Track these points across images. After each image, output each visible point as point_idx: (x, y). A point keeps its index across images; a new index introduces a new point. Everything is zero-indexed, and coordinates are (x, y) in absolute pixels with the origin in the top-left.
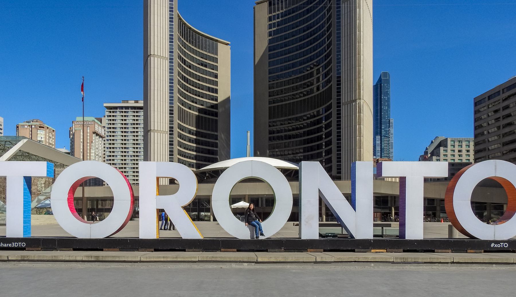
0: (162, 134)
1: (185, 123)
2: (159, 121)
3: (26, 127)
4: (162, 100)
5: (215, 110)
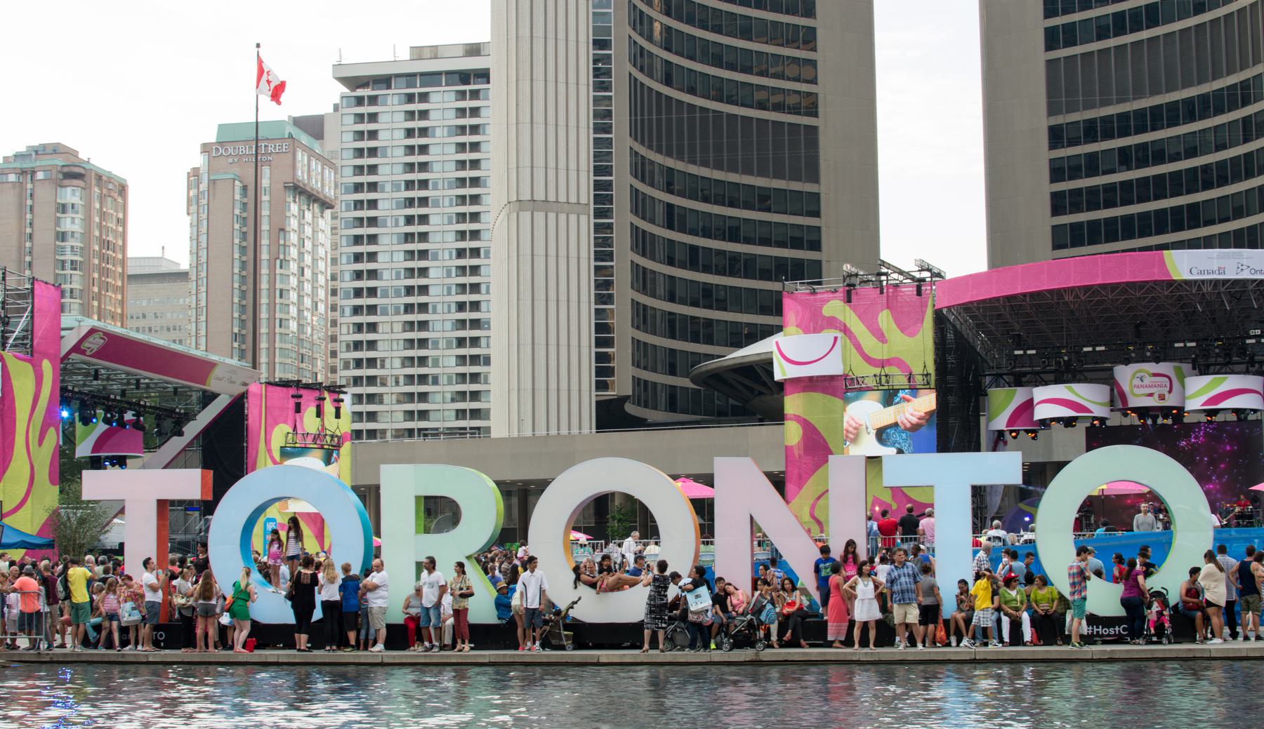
0: (563, 217)
1: (669, 154)
2: (552, 164)
4: (562, 78)
5: (804, 87)
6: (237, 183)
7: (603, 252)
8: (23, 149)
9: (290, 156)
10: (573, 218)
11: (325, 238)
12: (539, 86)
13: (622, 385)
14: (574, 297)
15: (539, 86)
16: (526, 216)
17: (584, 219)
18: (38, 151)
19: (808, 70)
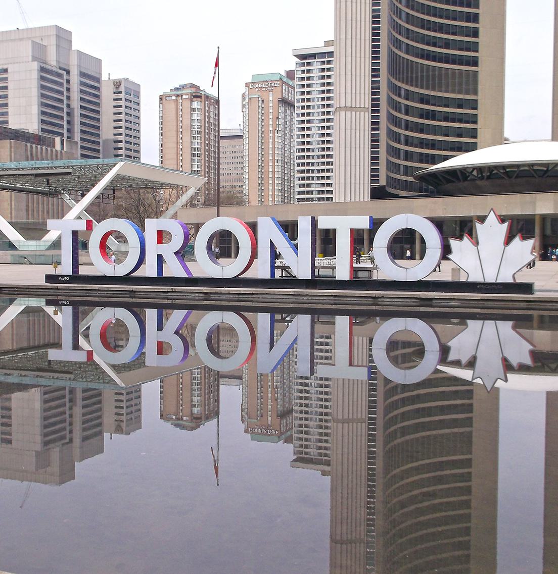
0: (358, 113)
2: (354, 91)
3: (173, 98)
6: (260, 99)
8: (178, 86)
9: (280, 87)
10: (362, 113)
12: (349, 59)
13: (383, 182)
14: (362, 146)
15: (349, 59)
17: (367, 114)
18: (183, 87)
19: (475, 47)
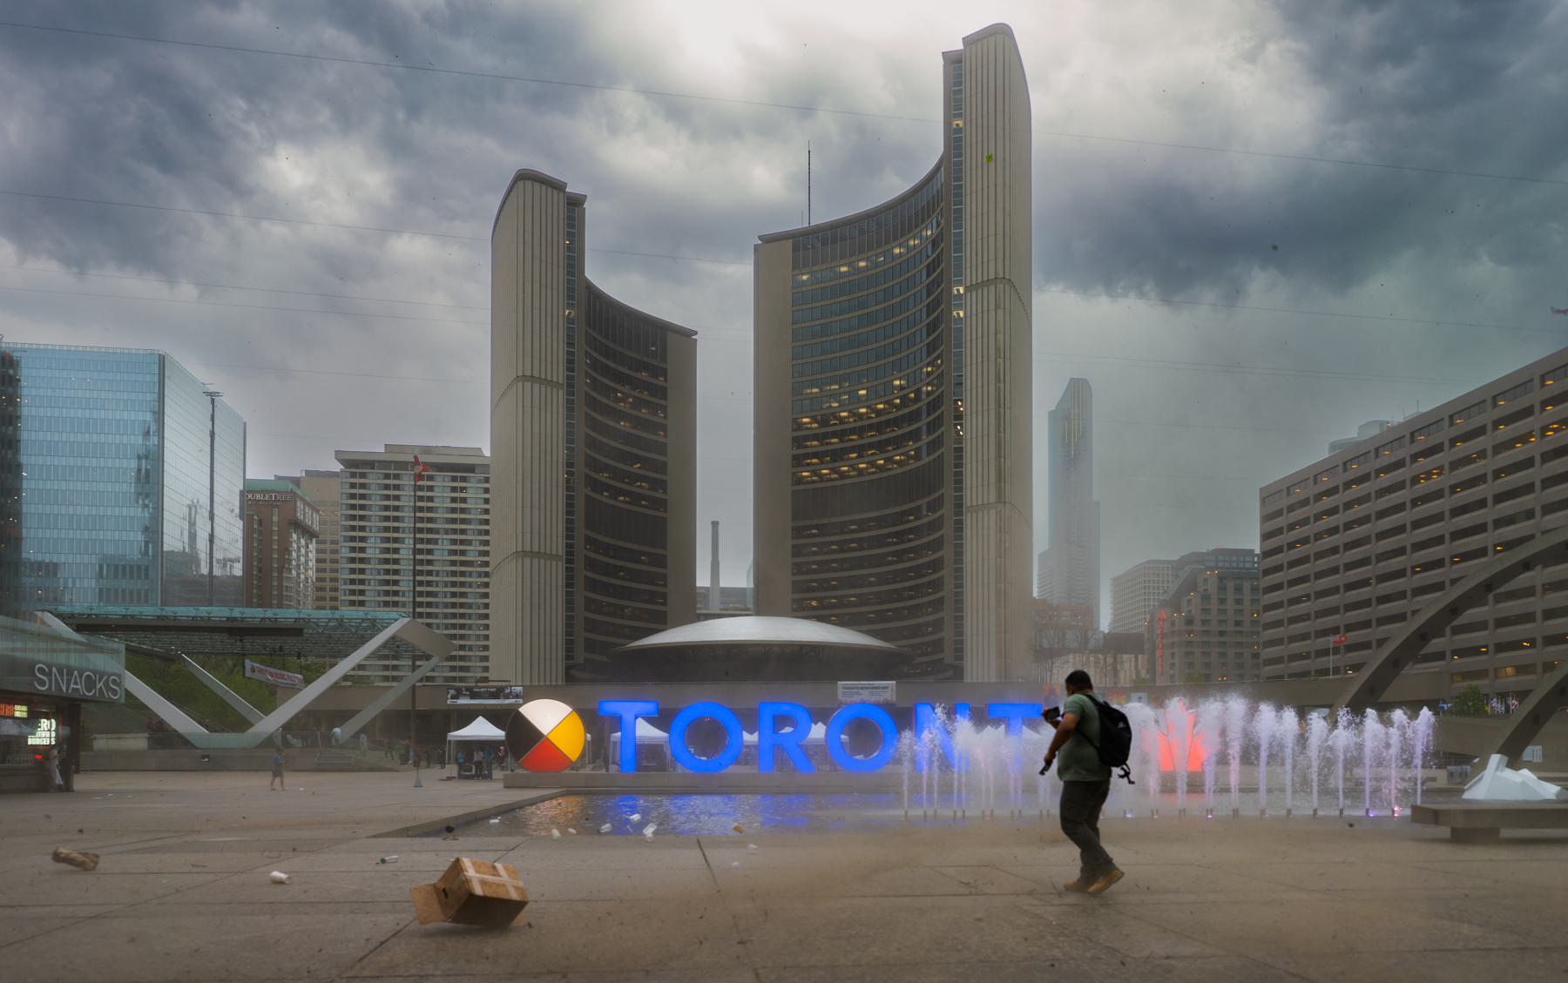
7: (569, 584)
11: (312, 556)
16: (527, 561)
